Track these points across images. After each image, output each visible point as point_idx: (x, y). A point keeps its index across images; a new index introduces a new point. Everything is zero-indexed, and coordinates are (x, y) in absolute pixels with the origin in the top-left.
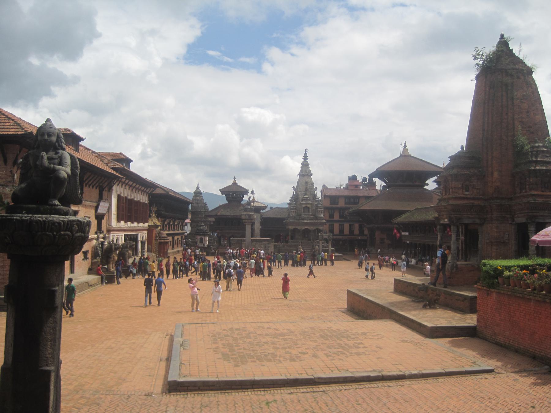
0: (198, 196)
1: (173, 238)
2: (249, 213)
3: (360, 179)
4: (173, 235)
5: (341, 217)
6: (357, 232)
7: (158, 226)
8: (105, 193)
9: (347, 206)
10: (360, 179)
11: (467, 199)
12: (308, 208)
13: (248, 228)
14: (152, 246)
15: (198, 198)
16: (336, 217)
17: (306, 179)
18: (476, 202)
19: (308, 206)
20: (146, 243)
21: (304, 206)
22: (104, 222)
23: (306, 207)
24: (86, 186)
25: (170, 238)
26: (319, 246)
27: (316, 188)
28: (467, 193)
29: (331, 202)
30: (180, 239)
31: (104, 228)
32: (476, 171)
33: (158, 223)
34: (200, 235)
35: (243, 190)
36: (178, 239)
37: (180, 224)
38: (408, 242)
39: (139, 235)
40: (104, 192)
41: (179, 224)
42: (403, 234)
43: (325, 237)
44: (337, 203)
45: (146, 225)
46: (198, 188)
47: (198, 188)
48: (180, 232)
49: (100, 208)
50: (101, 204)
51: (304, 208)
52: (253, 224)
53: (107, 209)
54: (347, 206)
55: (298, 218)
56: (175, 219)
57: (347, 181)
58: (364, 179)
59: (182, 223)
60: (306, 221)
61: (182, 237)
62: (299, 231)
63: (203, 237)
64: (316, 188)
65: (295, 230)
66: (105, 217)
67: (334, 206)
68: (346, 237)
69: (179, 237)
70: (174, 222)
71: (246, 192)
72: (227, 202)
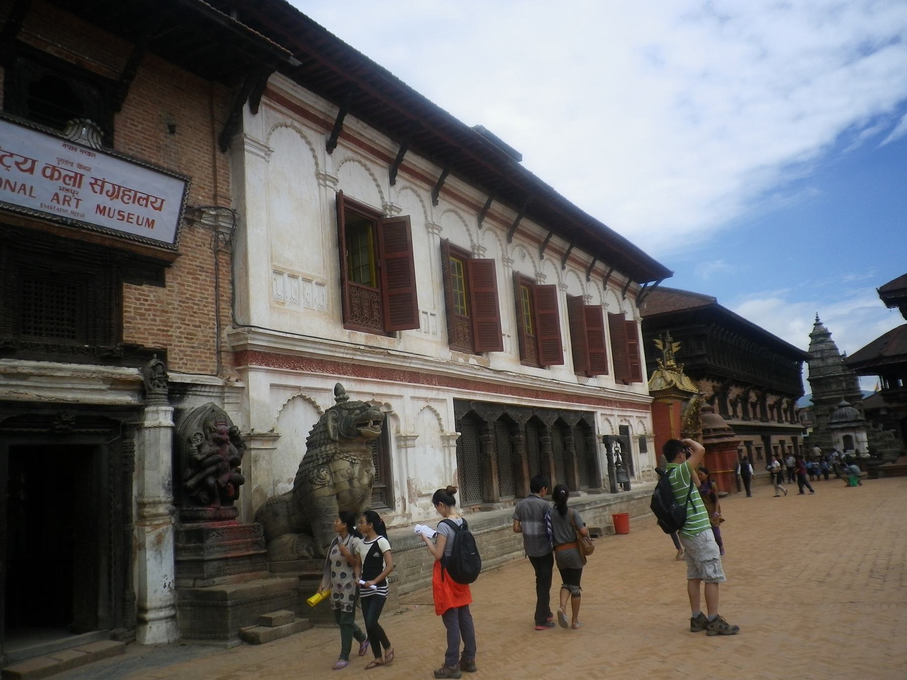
0: (822, 342)
1: (767, 440)
4: (766, 433)
7: (690, 394)
15: (822, 346)
25: (757, 440)
34: (842, 430)
36: (782, 442)
37: (785, 405)
41: (778, 404)
45: (641, 389)
46: (818, 324)
47: (818, 324)
48: (786, 425)
59: (791, 405)
61: (794, 440)
63: (851, 434)
69: (787, 439)
70: (762, 399)
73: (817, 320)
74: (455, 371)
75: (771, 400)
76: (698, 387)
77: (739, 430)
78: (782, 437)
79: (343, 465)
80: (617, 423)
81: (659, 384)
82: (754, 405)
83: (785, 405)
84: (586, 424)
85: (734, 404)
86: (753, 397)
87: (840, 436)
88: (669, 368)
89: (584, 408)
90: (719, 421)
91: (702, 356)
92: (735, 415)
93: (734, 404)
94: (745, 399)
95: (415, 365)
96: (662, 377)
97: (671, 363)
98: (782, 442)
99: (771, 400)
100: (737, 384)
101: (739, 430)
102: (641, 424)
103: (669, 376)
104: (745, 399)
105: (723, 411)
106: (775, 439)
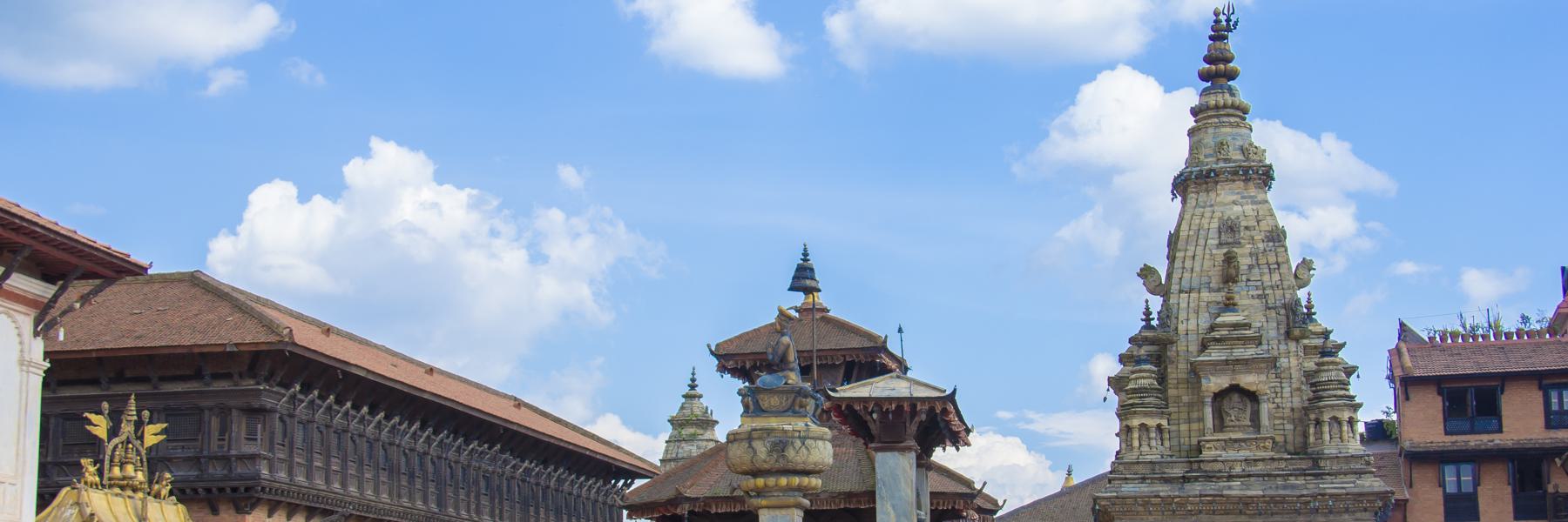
2: (773, 423)
12: (1252, 397)
17: (1229, 201)
19: (1248, 380)
23: (1235, 388)
27: (1306, 265)
35: (855, 343)
51: (1219, 396)
55: (1178, 471)
60: (1236, 489)
64: (1306, 265)
67: (1474, 441)
73: (693, 380)
91: (253, 458)
96: (77, 503)
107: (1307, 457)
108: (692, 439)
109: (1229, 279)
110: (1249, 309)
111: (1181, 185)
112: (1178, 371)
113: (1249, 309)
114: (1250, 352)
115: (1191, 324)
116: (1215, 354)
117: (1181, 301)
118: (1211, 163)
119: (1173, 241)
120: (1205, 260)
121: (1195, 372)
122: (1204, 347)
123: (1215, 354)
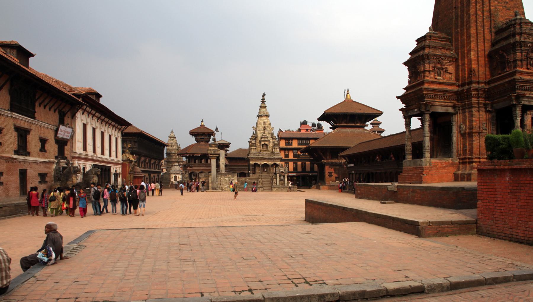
1: (150, 175)
3: (310, 124)
4: (150, 173)
5: (295, 156)
6: (308, 169)
8: (67, 120)
9: (300, 146)
10: (310, 124)
11: (440, 83)
12: (267, 145)
13: (213, 162)
14: (126, 179)
16: (291, 156)
17: (264, 119)
18: (450, 88)
19: (267, 143)
20: (121, 176)
21: (263, 143)
22: (67, 148)
24: (40, 106)
25: (147, 175)
26: (276, 179)
27: (273, 128)
28: (438, 78)
29: (286, 143)
30: (156, 177)
31: (67, 153)
32: (448, 53)
33: (132, 159)
34: (174, 174)
36: (154, 176)
37: (157, 163)
38: (353, 172)
39: (112, 168)
40: (66, 118)
41: (155, 163)
42: (349, 166)
43: (281, 170)
44: (291, 144)
48: (157, 170)
49: (59, 132)
50: (60, 129)
51: (263, 145)
52: (218, 160)
53: (70, 135)
54: (300, 146)
56: (151, 158)
57: (299, 126)
58: (313, 125)
59: (159, 163)
60: (265, 157)
61: (158, 176)
62: (258, 165)
64: (273, 128)
65: (255, 164)
66: (69, 144)
67: (289, 147)
68: (299, 174)
69: (156, 175)
70: (150, 161)
71: (211, 133)
72: (196, 142)
74: (94, 158)
75: (153, 161)
76: (133, 157)
77: (143, 172)
78: (154, 175)
79: (95, 178)
80: (115, 169)
81: (125, 158)
82: (147, 163)
83: (157, 163)
84: (109, 169)
85: (142, 163)
86: (147, 160)
87: (174, 175)
88: (127, 153)
89: (109, 165)
90: (138, 169)
92: (142, 167)
93: (142, 163)
94: (145, 161)
95: (90, 157)
97: (127, 151)
98: (154, 176)
99: (153, 161)
100: (144, 156)
101: (143, 172)
102: (119, 170)
103: (128, 155)
104: (145, 161)
105: (139, 166)
106: (152, 175)
107: (273, 153)
108: (172, 140)
109: (264, 130)
110: (267, 134)
111: (258, 116)
112: (258, 141)
113: (267, 134)
114: (266, 139)
115: (259, 135)
116: (263, 139)
117: (258, 132)
118: (262, 114)
119: (257, 124)
120: (261, 127)
121: (260, 141)
122: (261, 138)
123: (263, 139)
